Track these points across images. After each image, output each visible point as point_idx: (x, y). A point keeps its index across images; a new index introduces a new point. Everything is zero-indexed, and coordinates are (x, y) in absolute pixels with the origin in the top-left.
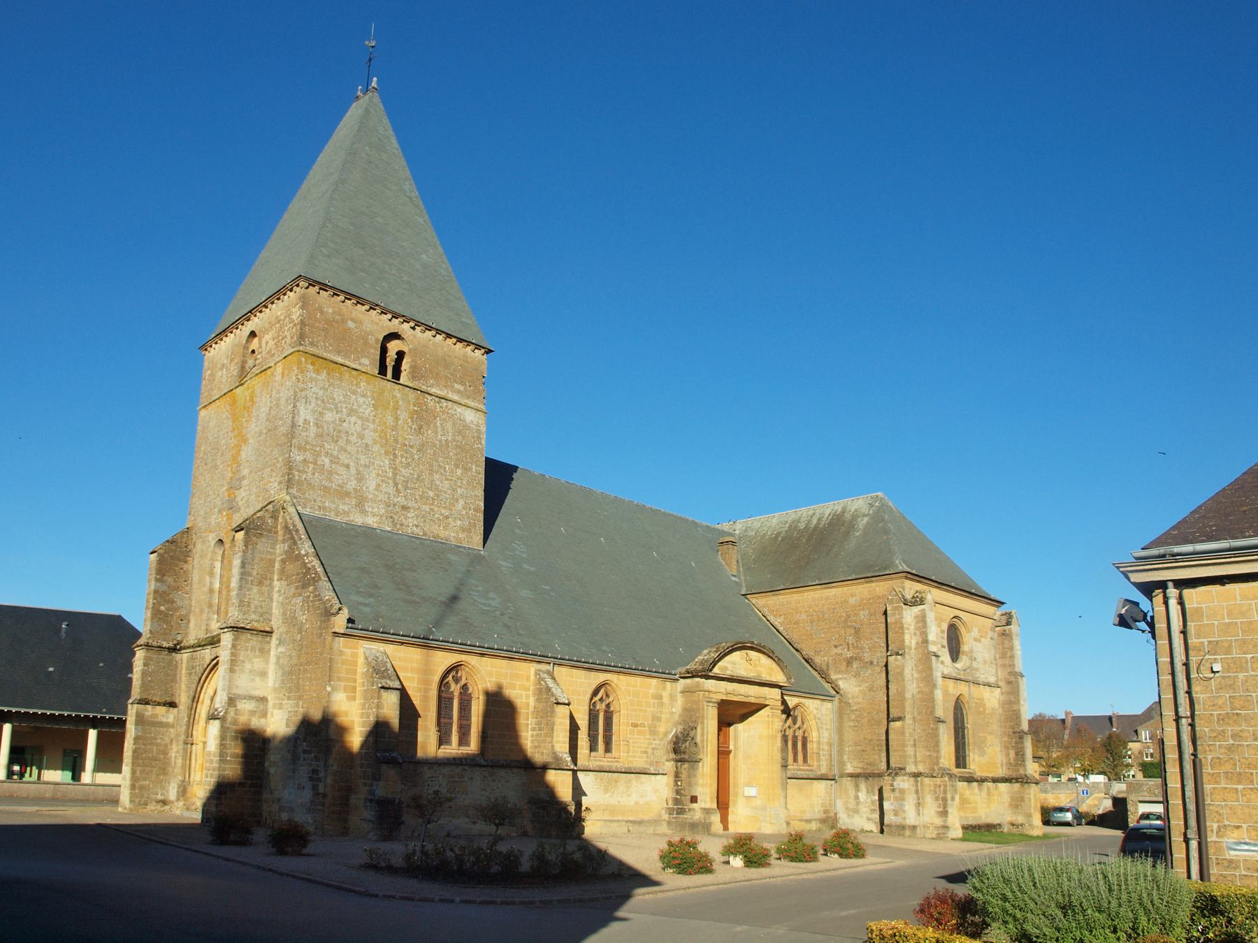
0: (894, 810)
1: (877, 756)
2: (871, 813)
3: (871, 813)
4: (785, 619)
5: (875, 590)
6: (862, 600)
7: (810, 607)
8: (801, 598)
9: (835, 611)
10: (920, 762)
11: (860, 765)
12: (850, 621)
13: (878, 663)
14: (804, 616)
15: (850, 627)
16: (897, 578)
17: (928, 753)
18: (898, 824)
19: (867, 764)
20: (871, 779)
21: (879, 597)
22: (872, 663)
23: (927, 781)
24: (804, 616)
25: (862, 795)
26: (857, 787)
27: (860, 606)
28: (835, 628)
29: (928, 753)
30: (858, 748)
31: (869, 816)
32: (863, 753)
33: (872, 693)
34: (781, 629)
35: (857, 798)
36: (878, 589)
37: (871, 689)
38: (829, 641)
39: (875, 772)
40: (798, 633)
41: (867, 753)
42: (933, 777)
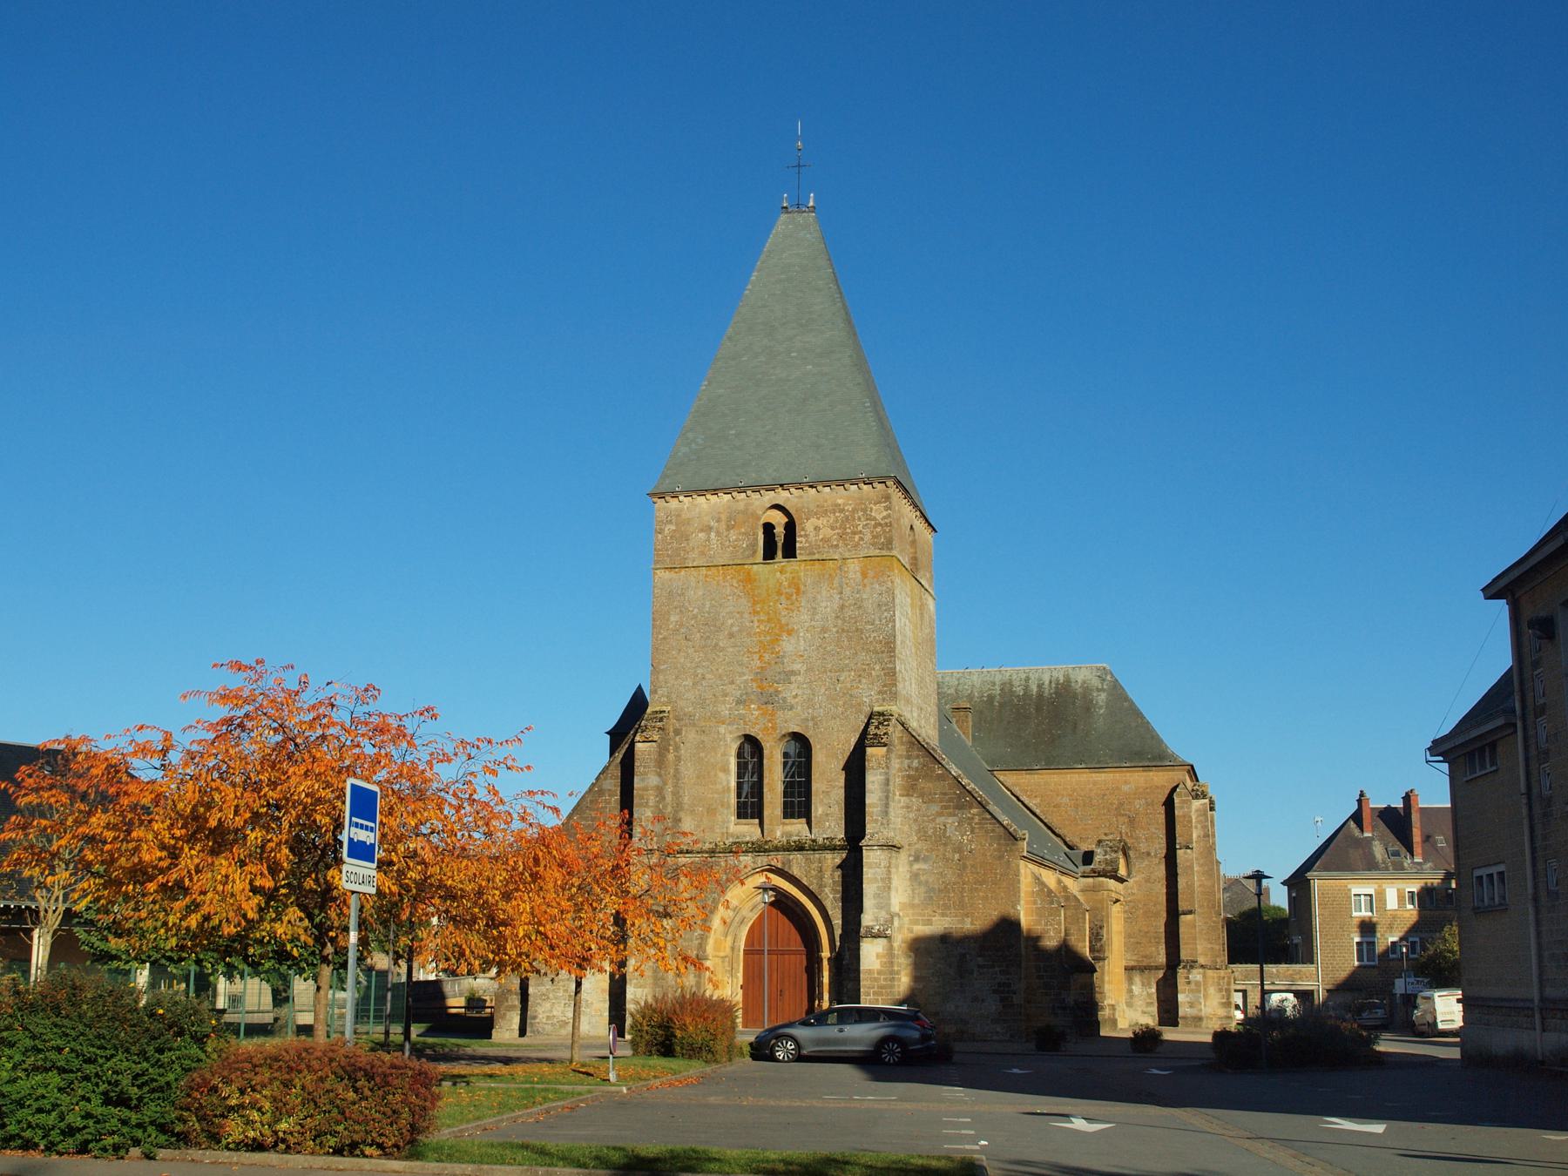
0: (1189, 1003)
1: (1154, 948)
2: (1147, 1007)
3: (1147, 1007)
4: (1041, 800)
5: (1152, 779)
6: (1137, 788)
7: (1074, 790)
8: (1062, 780)
9: (1105, 797)
10: (1201, 954)
11: (1134, 958)
12: (1124, 810)
13: (1156, 856)
14: (1066, 800)
15: (1123, 815)
16: (1178, 770)
17: (1209, 946)
18: (1194, 1015)
19: (1142, 957)
20: (1146, 972)
21: (1157, 787)
22: (1148, 854)
23: (1210, 973)
24: (1066, 800)
25: (1137, 989)
26: (1130, 981)
27: (1135, 794)
28: (1104, 814)
29: (1209, 946)
30: (1132, 940)
31: (1145, 1009)
32: (1139, 946)
33: (1149, 884)
34: (1038, 811)
35: (1130, 991)
36: (1156, 778)
37: (1148, 880)
38: (1098, 828)
39: (1152, 964)
40: (1059, 818)
41: (1142, 945)
42: (1217, 969)
